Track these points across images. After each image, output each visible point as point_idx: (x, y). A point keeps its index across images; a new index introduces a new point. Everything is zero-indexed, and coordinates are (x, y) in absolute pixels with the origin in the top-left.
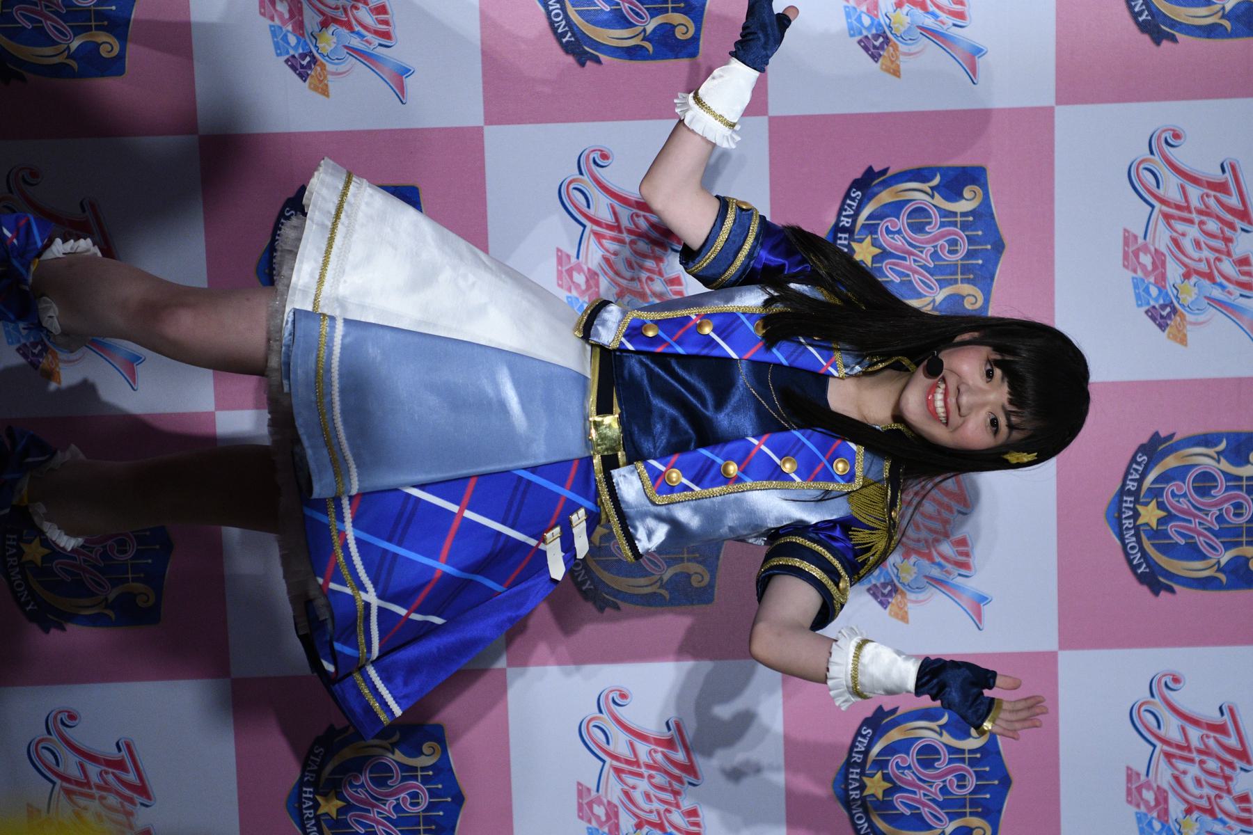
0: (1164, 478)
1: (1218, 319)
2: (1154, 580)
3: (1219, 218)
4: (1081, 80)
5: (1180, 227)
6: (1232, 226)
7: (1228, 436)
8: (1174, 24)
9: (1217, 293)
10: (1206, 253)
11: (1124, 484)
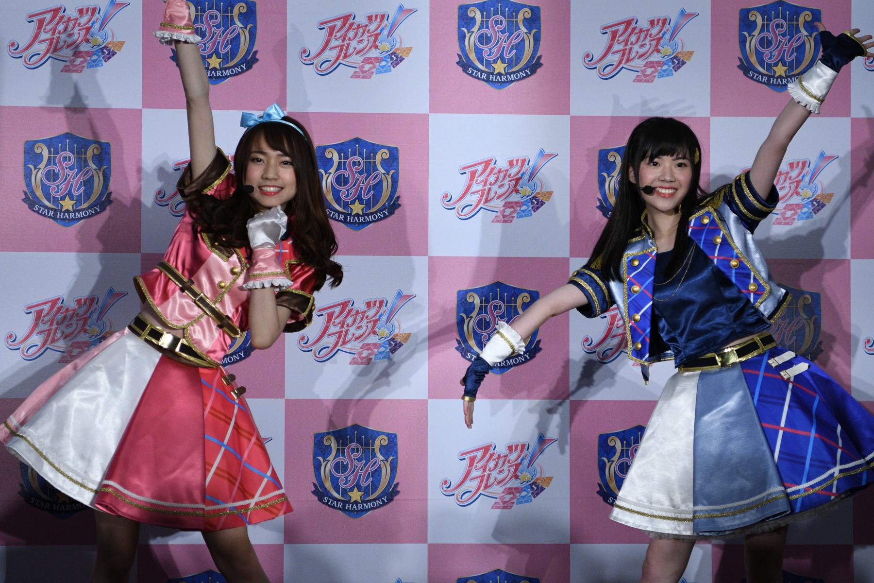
0: (761, 63)
1: (680, 36)
3: (630, 35)
4: (558, 103)
5: (633, 54)
6: (634, 29)
7: (741, 30)
8: (532, 57)
9: (667, 36)
10: (647, 41)
11: (764, 83)
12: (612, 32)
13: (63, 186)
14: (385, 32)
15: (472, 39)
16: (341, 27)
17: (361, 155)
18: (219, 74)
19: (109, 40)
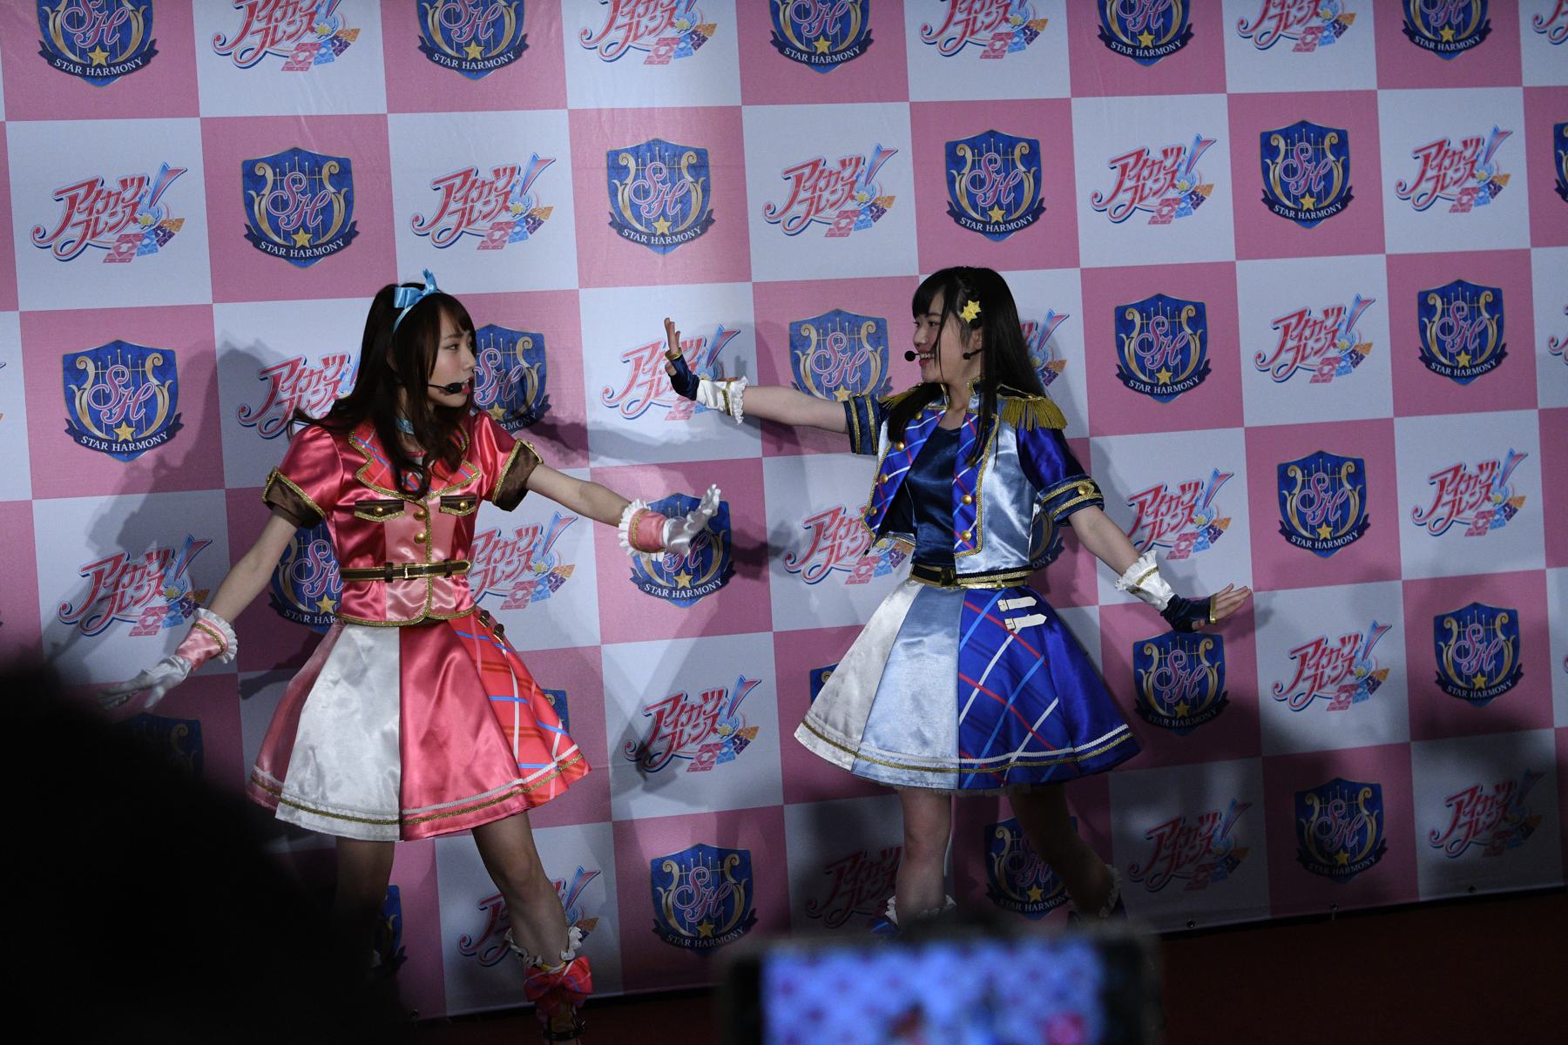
0: (975, 207)
2: (1036, 211)
4: (736, 266)
9: (862, 179)
12: (796, 176)
13: (117, 410)
14: (518, 189)
15: (625, 194)
16: (460, 188)
17: (497, 346)
18: (309, 253)
19: (164, 217)
